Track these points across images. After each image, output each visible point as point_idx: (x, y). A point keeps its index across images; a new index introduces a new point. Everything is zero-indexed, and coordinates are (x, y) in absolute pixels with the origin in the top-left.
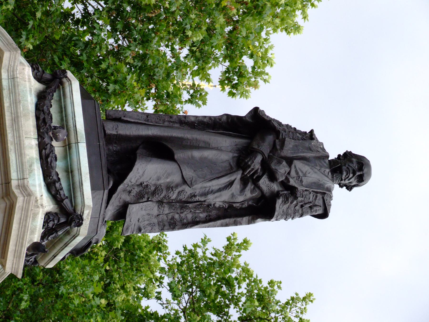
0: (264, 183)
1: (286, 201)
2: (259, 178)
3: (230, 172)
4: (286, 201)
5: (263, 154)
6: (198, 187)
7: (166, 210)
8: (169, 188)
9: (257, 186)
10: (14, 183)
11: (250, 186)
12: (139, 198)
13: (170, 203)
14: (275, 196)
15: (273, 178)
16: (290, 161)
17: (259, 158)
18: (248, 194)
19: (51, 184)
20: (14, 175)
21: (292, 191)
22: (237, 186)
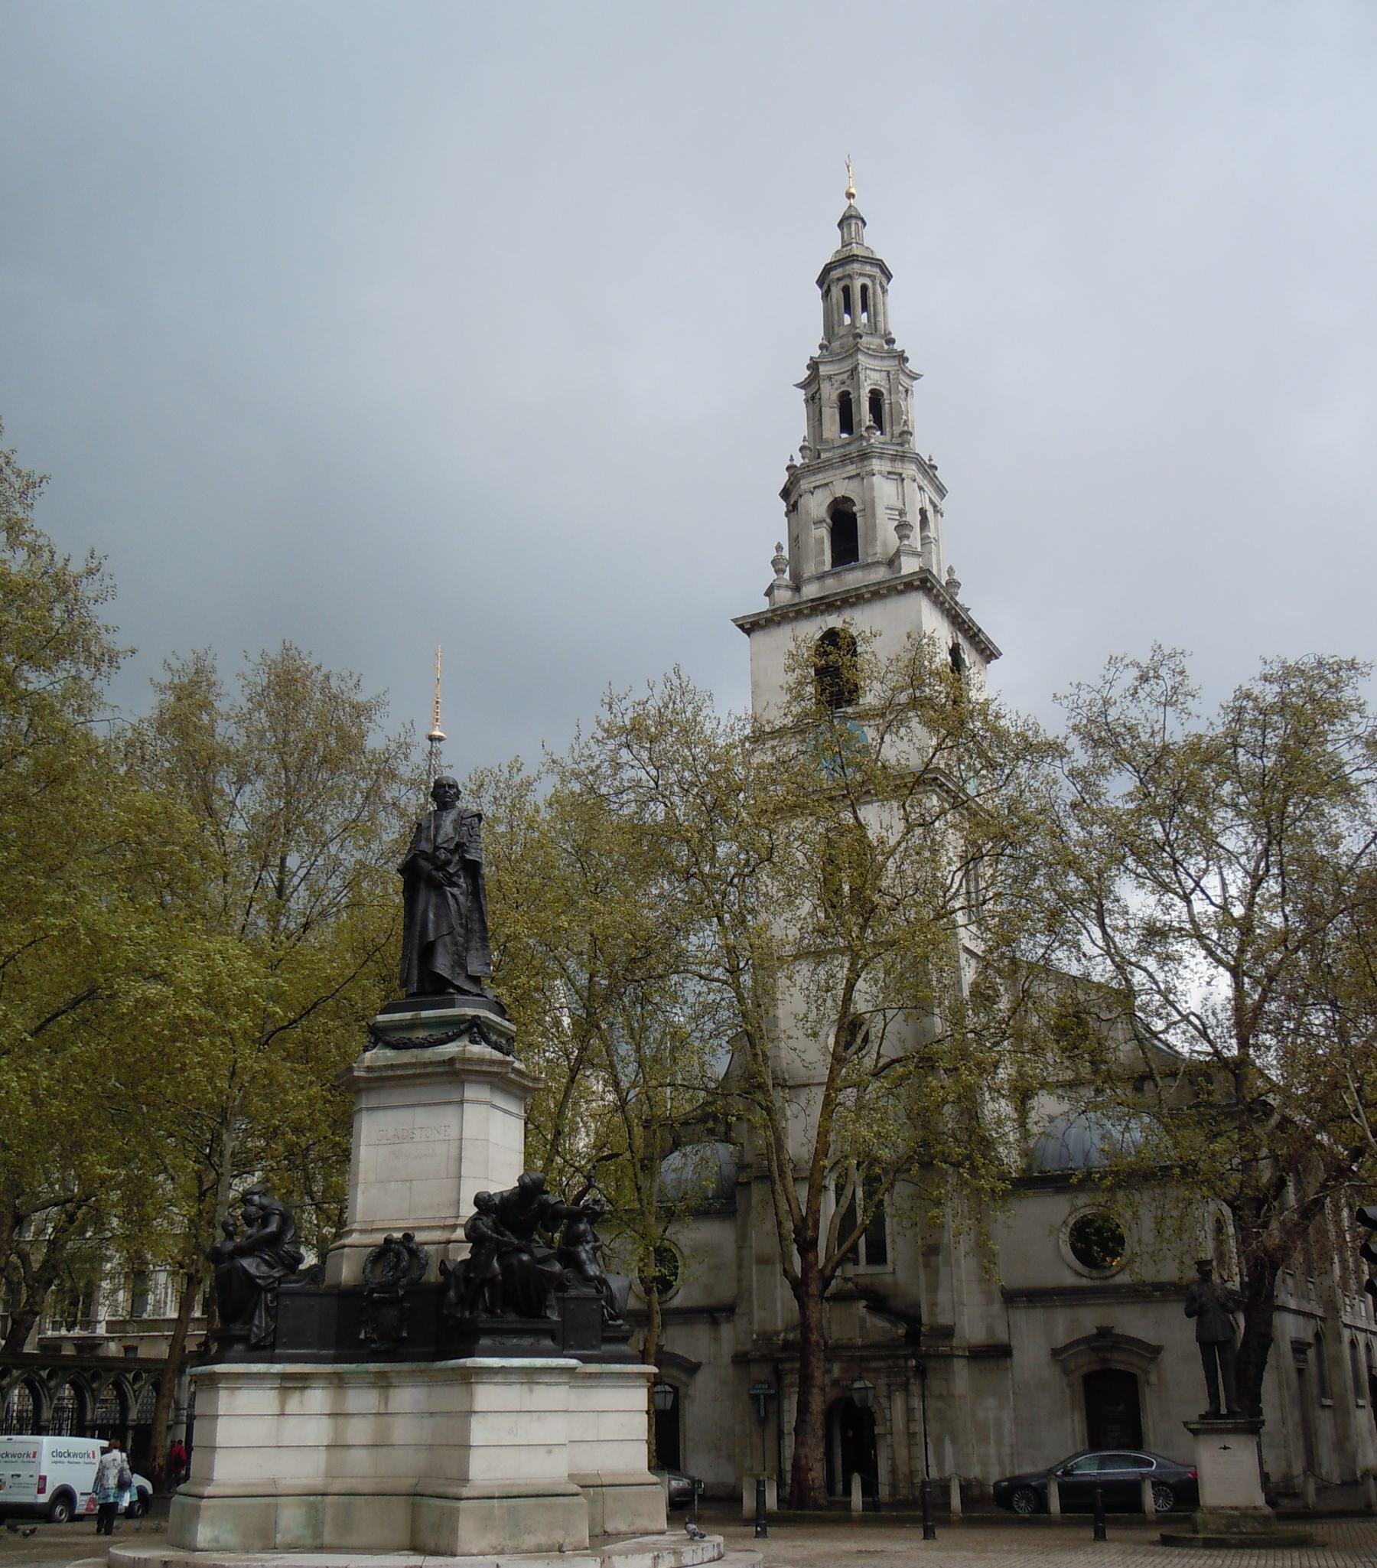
1: (467, 852)
3: (443, 896)
4: (467, 852)
6: (455, 921)
7: (473, 944)
9: (456, 874)
11: (455, 879)
12: (464, 967)
13: (468, 941)
14: (462, 859)
15: (448, 862)
16: (437, 848)
17: (434, 873)
19: (450, 1039)
20: (440, 1070)
21: (460, 846)
22: (455, 891)
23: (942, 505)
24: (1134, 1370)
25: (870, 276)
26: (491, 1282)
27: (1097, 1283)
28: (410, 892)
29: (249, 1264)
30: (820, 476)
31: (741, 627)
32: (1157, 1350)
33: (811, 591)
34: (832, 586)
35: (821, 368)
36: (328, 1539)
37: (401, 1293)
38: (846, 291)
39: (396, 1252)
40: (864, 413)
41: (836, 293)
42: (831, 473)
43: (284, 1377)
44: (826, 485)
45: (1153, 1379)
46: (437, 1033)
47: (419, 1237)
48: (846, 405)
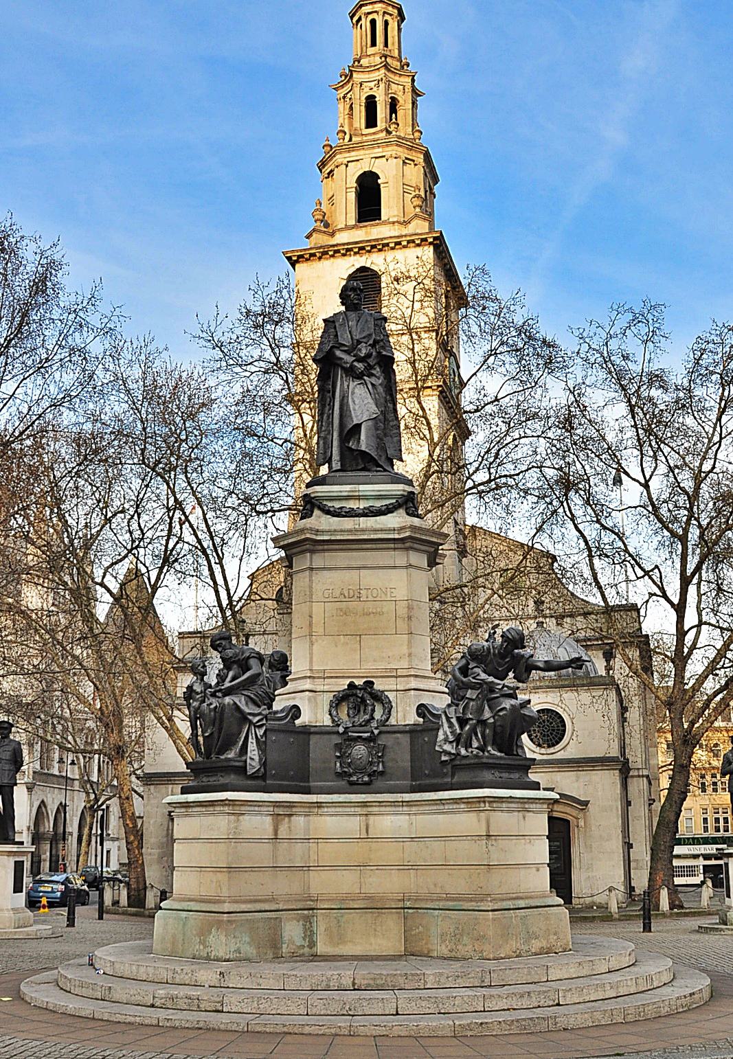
0: (372, 361)
2: (369, 365)
5: (354, 361)
8: (377, 429)
10: (397, 536)
17: (355, 364)
18: (377, 371)
19: (388, 510)
21: (376, 342)
22: (373, 380)
23: (436, 189)
24: (569, 818)
25: (391, 15)
26: (483, 723)
27: (545, 757)
28: (326, 377)
29: (241, 701)
30: (353, 154)
31: (289, 259)
32: (586, 803)
33: (342, 238)
34: (360, 235)
35: (355, 75)
36: (321, 948)
37: (376, 732)
38: (373, 22)
39: (359, 697)
40: (382, 112)
41: (366, 23)
42: (362, 152)
43: (276, 804)
44: (358, 160)
45: (582, 823)
46: (378, 504)
47: (378, 685)
48: (371, 103)
